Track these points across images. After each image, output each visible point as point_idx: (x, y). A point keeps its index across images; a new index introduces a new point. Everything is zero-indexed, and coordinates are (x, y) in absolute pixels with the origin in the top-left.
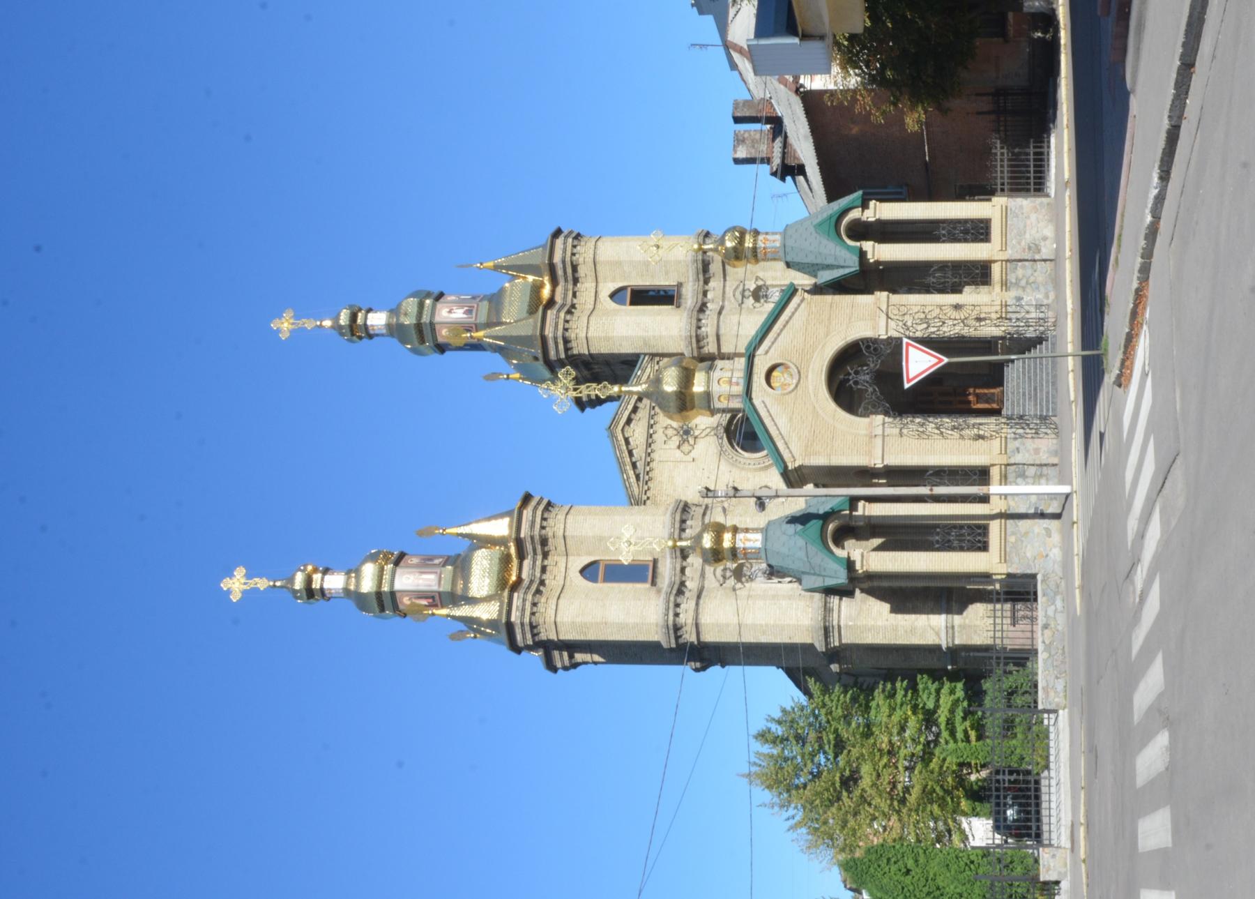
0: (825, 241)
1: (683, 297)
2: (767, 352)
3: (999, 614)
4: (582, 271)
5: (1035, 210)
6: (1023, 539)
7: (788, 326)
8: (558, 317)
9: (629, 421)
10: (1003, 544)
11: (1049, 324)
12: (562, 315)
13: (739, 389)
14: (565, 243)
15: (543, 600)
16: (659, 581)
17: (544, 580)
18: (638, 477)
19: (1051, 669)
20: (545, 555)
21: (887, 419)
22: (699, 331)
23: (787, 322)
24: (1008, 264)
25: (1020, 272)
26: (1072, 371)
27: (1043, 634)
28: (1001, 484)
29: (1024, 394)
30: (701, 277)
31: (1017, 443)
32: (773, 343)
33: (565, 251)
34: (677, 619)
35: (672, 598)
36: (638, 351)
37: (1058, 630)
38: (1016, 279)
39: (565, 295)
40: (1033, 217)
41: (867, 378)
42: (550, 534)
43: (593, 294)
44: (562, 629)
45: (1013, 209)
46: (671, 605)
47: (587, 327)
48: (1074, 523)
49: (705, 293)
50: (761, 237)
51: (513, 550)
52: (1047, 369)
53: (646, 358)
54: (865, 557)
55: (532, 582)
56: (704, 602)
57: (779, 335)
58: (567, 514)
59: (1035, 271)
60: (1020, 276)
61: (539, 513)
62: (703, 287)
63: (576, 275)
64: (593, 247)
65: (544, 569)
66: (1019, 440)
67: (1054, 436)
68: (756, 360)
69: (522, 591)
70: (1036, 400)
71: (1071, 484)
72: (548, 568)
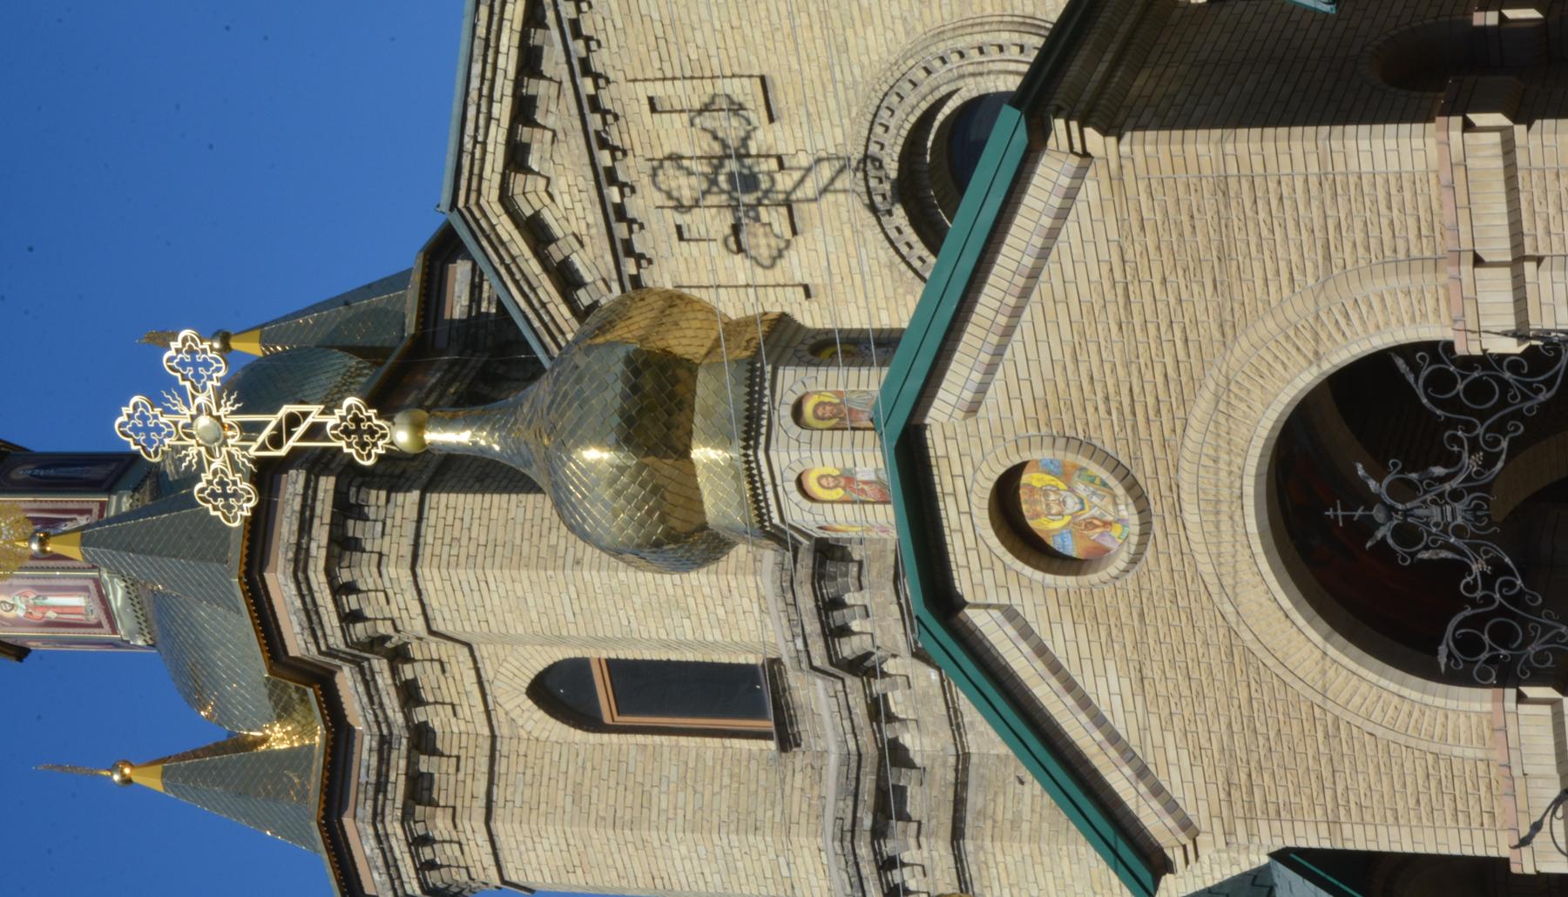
7: (1042, 286)
9: (517, 157)
35: (864, 851)
41: (1458, 513)
46: (868, 870)
55: (385, 744)
65: (410, 694)
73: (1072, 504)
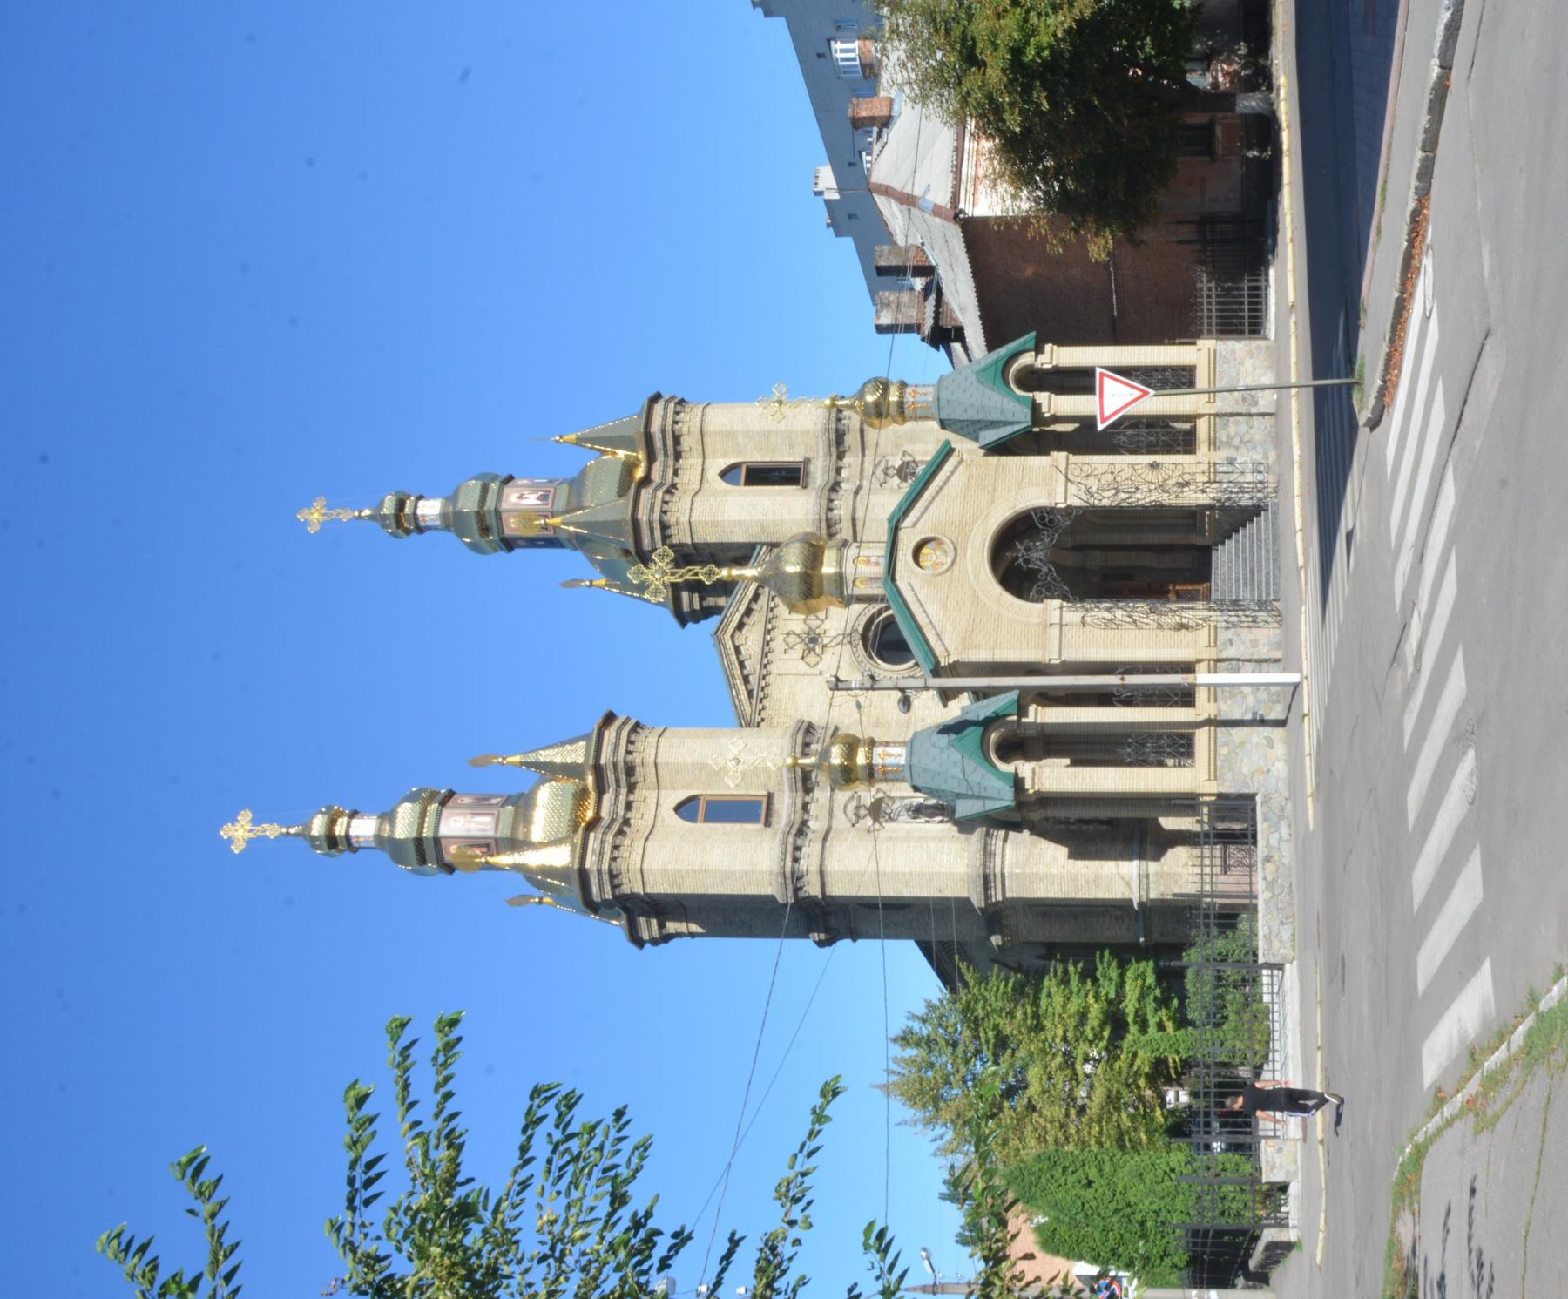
0: (988, 392)
1: (811, 475)
2: (915, 524)
3: (1207, 862)
4: (686, 443)
5: (1251, 355)
6: (1238, 750)
8: (654, 497)
9: (740, 626)
10: (1212, 756)
11: (1269, 490)
12: (660, 494)
13: (880, 570)
14: (665, 409)
15: (627, 842)
16: (774, 820)
17: (629, 819)
18: (750, 693)
19: (1275, 912)
20: (631, 788)
21: (1065, 604)
22: (830, 514)
23: (941, 488)
24: (1218, 419)
25: (1232, 429)
26: (1301, 530)
27: (1264, 869)
28: (1209, 672)
29: (1237, 580)
30: (834, 450)
31: (1230, 634)
32: (923, 513)
33: (665, 418)
34: (797, 865)
35: (791, 839)
36: (754, 540)
37: (1283, 864)
38: (1228, 437)
39: (664, 472)
40: (1248, 363)
41: (1041, 555)
42: (638, 761)
43: (699, 472)
44: (649, 879)
45: (1223, 353)
46: (790, 848)
47: (691, 510)
48: (1305, 715)
49: (838, 471)
50: (909, 390)
51: (590, 780)
52: (1266, 544)
53: (764, 548)
54: (1037, 774)
55: (613, 821)
56: (831, 845)
57: (930, 503)
58: (660, 736)
59: (1251, 428)
60: (1233, 434)
61: (624, 734)
62: (837, 463)
63: (679, 449)
64: (700, 415)
65: (629, 806)
66: (1233, 630)
67: (1276, 625)
68: (902, 534)
69: (600, 831)
70: (1253, 585)
71: (1300, 670)
72: (635, 805)
73: (934, 558)
